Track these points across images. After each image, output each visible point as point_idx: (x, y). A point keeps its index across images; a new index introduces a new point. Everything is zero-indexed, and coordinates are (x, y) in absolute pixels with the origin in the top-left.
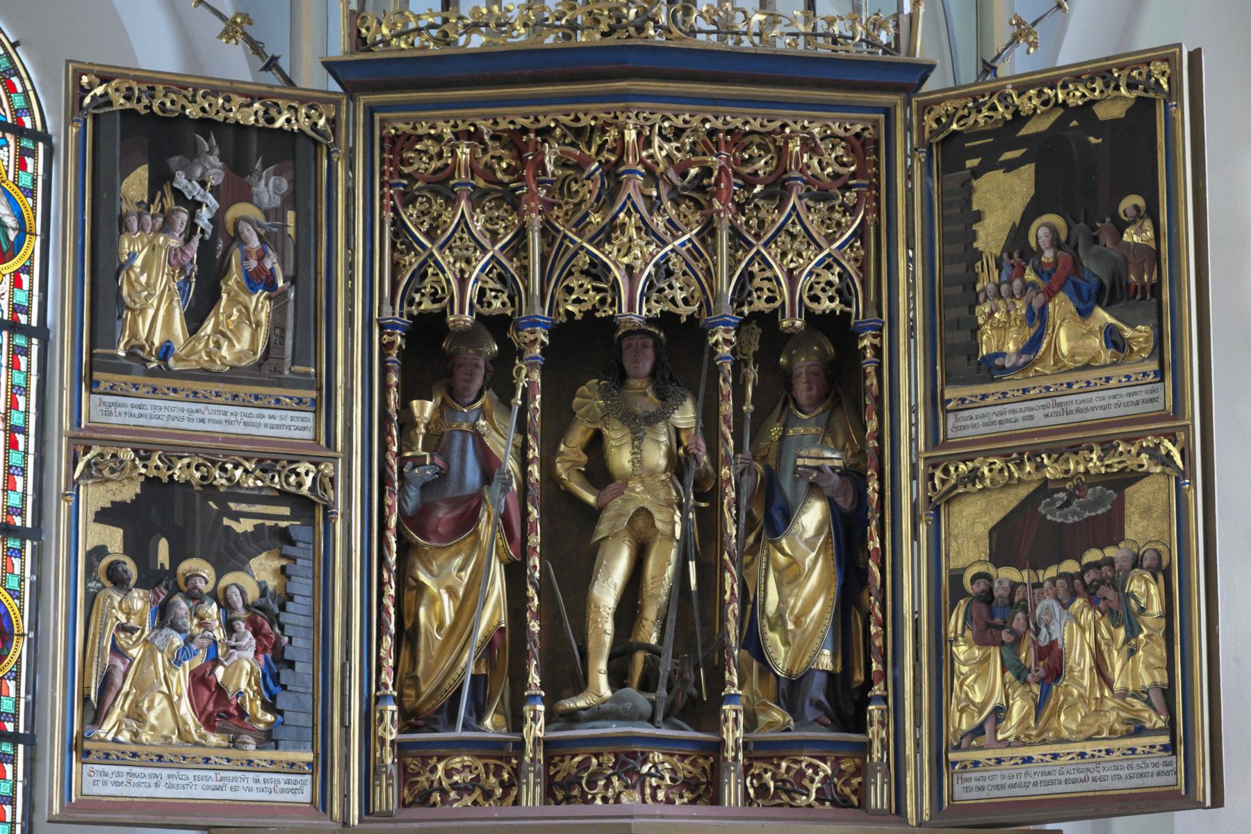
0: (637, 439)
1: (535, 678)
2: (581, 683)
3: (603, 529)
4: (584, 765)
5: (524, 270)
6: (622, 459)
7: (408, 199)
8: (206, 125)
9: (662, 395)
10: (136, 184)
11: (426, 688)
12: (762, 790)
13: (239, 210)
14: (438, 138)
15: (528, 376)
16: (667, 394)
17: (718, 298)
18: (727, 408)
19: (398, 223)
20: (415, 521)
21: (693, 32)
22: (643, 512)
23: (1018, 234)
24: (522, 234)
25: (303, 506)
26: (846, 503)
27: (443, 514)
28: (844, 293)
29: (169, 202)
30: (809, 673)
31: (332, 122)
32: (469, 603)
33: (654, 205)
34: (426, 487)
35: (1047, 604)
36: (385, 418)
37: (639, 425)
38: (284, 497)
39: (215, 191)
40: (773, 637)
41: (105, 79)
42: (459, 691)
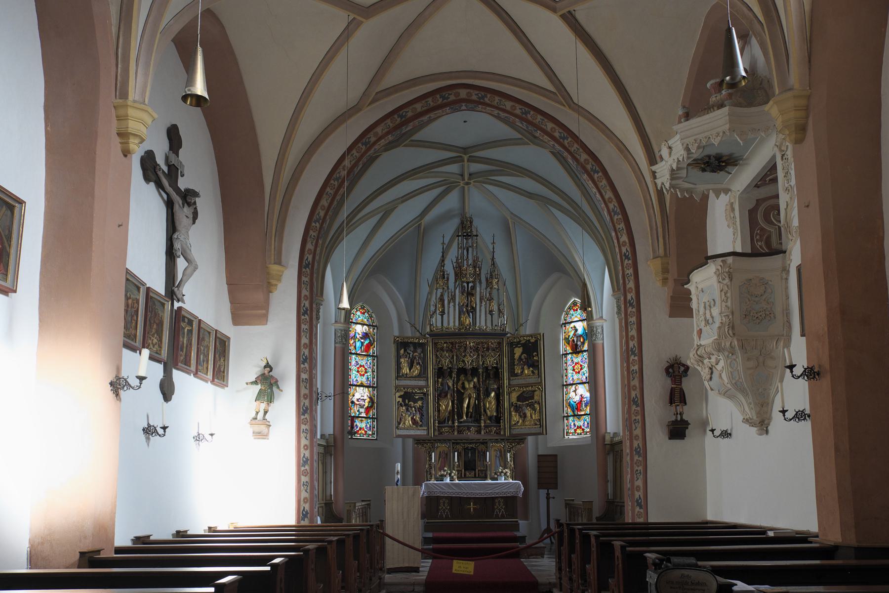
0: (469, 384)
1: (456, 417)
2: (462, 417)
3: (465, 396)
4: (463, 429)
5: (453, 361)
6: (467, 386)
7: (438, 351)
8: (411, 343)
9: (472, 377)
10: (402, 351)
11: (441, 418)
12: (487, 432)
13: (415, 354)
14: (442, 343)
15: (454, 375)
16: (473, 377)
17: (480, 364)
18: (481, 380)
19: (436, 355)
20: (439, 395)
21: (476, 329)
22: (470, 394)
23: (520, 357)
24: (453, 356)
25: (424, 394)
26: (497, 392)
27: (443, 394)
28: (497, 364)
29: (406, 354)
30: (493, 416)
31: (427, 341)
32: (447, 406)
33: (471, 352)
34: (440, 391)
35: (524, 407)
36: (435, 382)
37: (469, 382)
38: (422, 393)
39: (412, 352)
40: (488, 411)
41: (398, 338)
42: (446, 418)
